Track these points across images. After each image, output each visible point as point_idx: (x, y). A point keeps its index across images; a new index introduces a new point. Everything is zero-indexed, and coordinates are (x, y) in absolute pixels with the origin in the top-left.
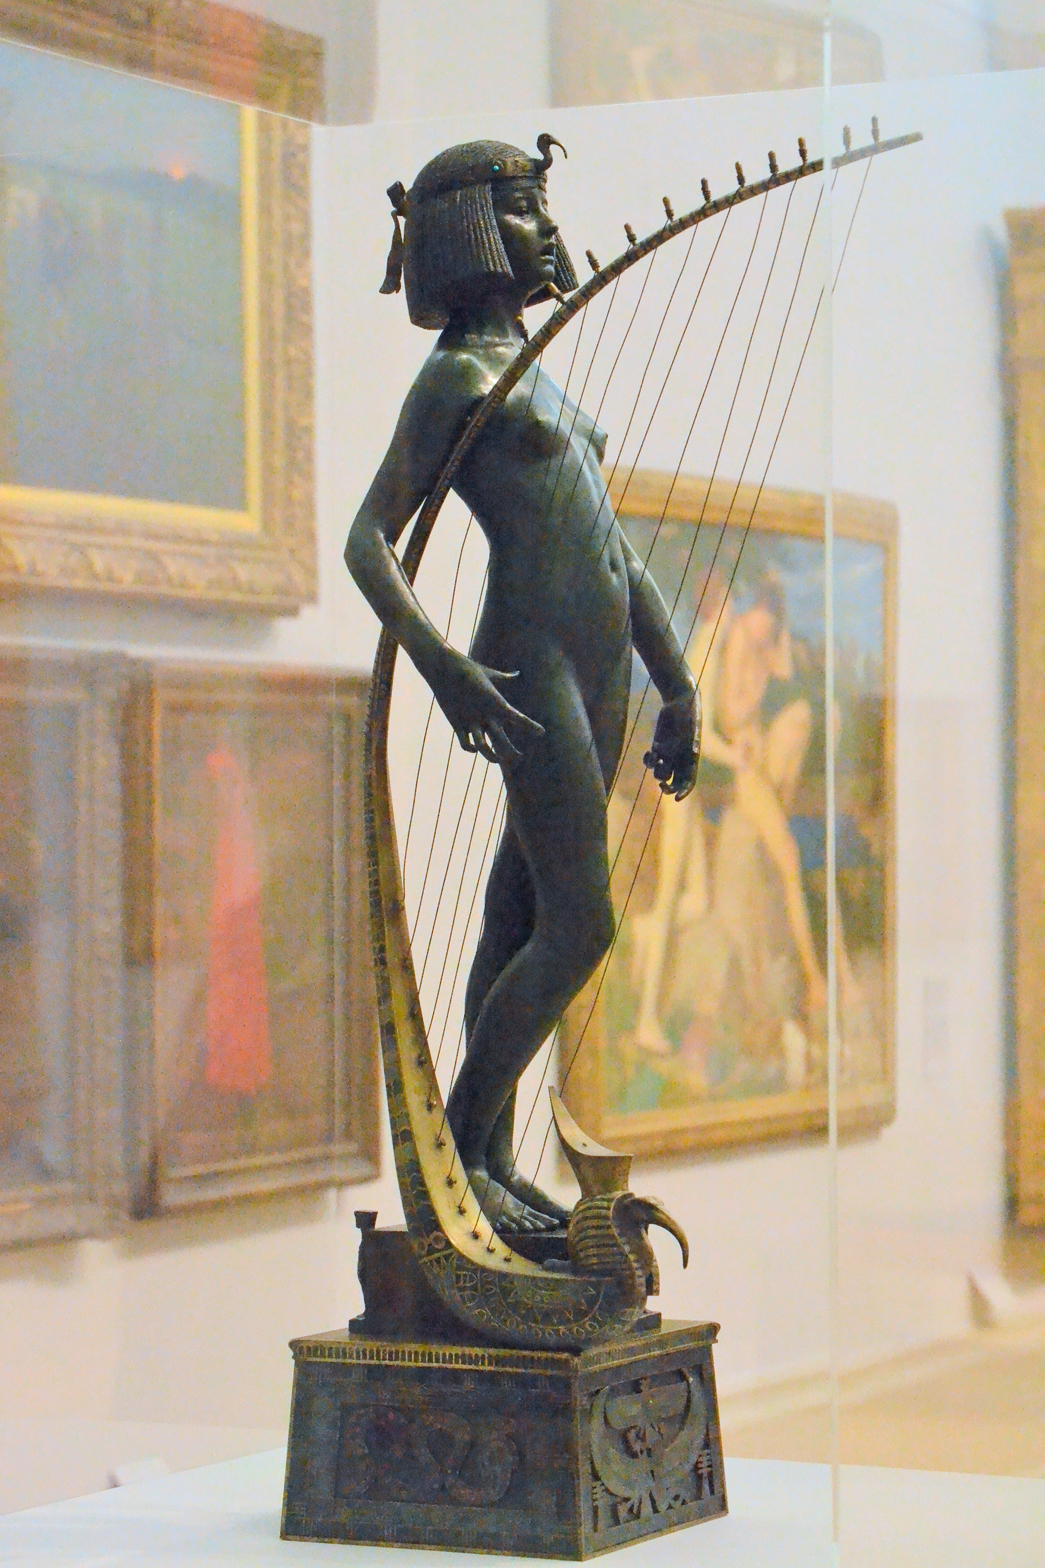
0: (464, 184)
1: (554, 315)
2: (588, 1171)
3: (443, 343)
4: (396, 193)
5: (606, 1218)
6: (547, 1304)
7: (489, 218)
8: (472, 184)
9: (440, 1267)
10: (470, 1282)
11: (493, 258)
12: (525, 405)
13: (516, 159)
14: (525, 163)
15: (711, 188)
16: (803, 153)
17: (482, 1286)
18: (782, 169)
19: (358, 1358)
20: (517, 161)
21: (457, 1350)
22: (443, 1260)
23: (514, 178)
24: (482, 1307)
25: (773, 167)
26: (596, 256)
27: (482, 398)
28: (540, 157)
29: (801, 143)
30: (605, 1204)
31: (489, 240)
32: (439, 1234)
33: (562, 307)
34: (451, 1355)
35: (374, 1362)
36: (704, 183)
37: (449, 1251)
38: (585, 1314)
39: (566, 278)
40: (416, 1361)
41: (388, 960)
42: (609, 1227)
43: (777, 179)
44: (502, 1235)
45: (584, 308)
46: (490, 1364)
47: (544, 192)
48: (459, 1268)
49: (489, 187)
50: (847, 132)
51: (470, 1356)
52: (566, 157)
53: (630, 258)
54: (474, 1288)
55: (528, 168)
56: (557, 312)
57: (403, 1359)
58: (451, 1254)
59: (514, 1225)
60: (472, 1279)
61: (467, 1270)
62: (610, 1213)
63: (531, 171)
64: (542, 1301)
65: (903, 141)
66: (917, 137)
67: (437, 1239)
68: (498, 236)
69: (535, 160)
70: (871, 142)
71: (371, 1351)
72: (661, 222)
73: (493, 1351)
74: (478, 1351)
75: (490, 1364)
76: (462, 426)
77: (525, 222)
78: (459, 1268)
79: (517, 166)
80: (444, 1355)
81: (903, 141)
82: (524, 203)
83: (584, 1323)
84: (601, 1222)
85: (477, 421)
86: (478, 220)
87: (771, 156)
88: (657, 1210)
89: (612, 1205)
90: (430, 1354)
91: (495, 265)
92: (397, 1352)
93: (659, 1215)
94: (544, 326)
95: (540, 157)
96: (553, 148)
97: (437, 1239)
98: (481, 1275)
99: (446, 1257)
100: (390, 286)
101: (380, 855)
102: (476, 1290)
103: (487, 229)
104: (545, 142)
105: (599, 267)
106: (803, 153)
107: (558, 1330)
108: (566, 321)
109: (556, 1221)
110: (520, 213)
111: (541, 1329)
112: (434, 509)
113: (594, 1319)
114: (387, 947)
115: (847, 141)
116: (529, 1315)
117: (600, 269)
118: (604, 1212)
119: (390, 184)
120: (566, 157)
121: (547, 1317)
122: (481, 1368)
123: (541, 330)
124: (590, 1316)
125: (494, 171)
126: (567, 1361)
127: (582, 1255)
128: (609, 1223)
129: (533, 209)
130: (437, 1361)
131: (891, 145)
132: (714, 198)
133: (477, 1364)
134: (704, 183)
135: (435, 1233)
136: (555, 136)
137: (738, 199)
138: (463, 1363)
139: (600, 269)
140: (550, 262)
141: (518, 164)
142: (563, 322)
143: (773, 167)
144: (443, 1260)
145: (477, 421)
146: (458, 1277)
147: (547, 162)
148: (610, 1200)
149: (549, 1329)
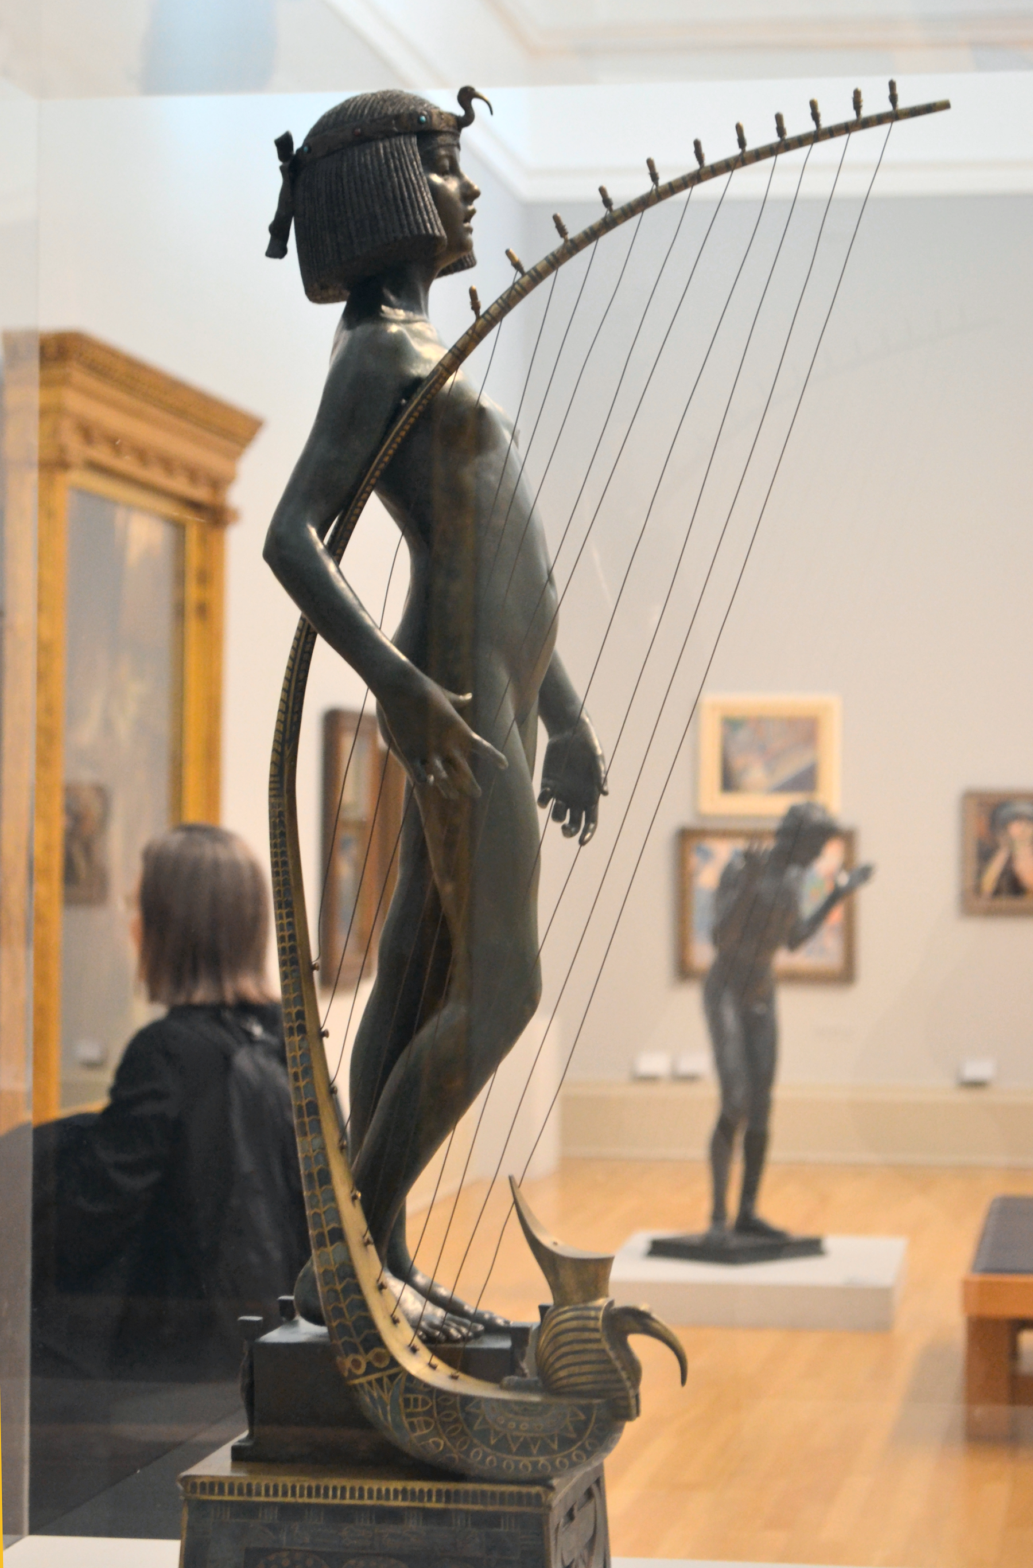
0: (388, 135)
1: (514, 284)
2: (568, 1277)
3: (350, 319)
4: (284, 144)
5: (596, 1330)
6: (526, 1431)
8: (399, 134)
9: (383, 1390)
10: (423, 1406)
11: (430, 219)
12: (459, 391)
15: (705, 150)
16: (815, 116)
17: (438, 1413)
18: (792, 131)
19: (267, 1494)
21: (398, 1485)
22: (385, 1380)
23: (439, 133)
24: (439, 1435)
25: (781, 131)
26: (564, 221)
27: (418, 381)
28: (460, 112)
29: (813, 105)
30: (593, 1313)
32: (383, 1351)
34: (388, 1491)
35: (289, 1499)
36: (697, 144)
38: (572, 1442)
40: (343, 1497)
41: (308, 1029)
42: (598, 1341)
43: (785, 145)
44: (433, 1346)
46: (438, 1501)
48: (408, 1390)
49: (414, 140)
50: (857, 96)
51: (413, 1492)
52: (492, 113)
53: (608, 224)
54: (429, 1413)
57: (326, 1496)
58: (396, 1375)
59: (438, 1333)
60: (425, 1403)
62: (600, 1323)
64: (517, 1428)
66: (945, 106)
68: (430, 196)
70: (887, 107)
71: (285, 1486)
72: (645, 186)
73: (444, 1486)
74: (425, 1486)
75: (438, 1501)
76: (398, 411)
78: (408, 1390)
79: (442, 119)
80: (379, 1491)
82: (447, 163)
83: (572, 1453)
84: (586, 1335)
85: (414, 405)
87: (779, 118)
88: (653, 1319)
89: (601, 1314)
90: (361, 1489)
92: (318, 1488)
93: (654, 1325)
94: (501, 297)
95: (460, 112)
96: (475, 103)
97: (379, 1358)
98: (437, 1398)
99: (392, 1378)
100: (276, 250)
101: (294, 904)
102: (432, 1417)
103: (420, 187)
104: (466, 96)
106: (815, 116)
107: (537, 1463)
109: (480, 1327)
110: (442, 173)
111: (484, 1452)
112: (360, 504)
113: (582, 1448)
114: (306, 1013)
116: (502, 1445)
117: (570, 236)
118: (592, 1324)
119: (279, 134)
121: (524, 1449)
122: (428, 1505)
123: (497, 302)
124: (579, 1443)
125: (420, 122)
126: (538, 1496)
127: (562, 1374)
128: (597, 1335)
129: (453, 170)
130: (371, 1497)
132: (709, 160)
133: (421, 1500)
134: (697, 144)
135: (377, 1350)
136: (478, 90)
137: (740, 163)
138: (404, 1499)
139: (570, 236)
141: (443, 117)
143: (781, 131)
144: (385, 1380)
145: (414, 405)
146: (407, 1401)
147: (468, 119)
148: (598, 1309)
149: (525, 1461)
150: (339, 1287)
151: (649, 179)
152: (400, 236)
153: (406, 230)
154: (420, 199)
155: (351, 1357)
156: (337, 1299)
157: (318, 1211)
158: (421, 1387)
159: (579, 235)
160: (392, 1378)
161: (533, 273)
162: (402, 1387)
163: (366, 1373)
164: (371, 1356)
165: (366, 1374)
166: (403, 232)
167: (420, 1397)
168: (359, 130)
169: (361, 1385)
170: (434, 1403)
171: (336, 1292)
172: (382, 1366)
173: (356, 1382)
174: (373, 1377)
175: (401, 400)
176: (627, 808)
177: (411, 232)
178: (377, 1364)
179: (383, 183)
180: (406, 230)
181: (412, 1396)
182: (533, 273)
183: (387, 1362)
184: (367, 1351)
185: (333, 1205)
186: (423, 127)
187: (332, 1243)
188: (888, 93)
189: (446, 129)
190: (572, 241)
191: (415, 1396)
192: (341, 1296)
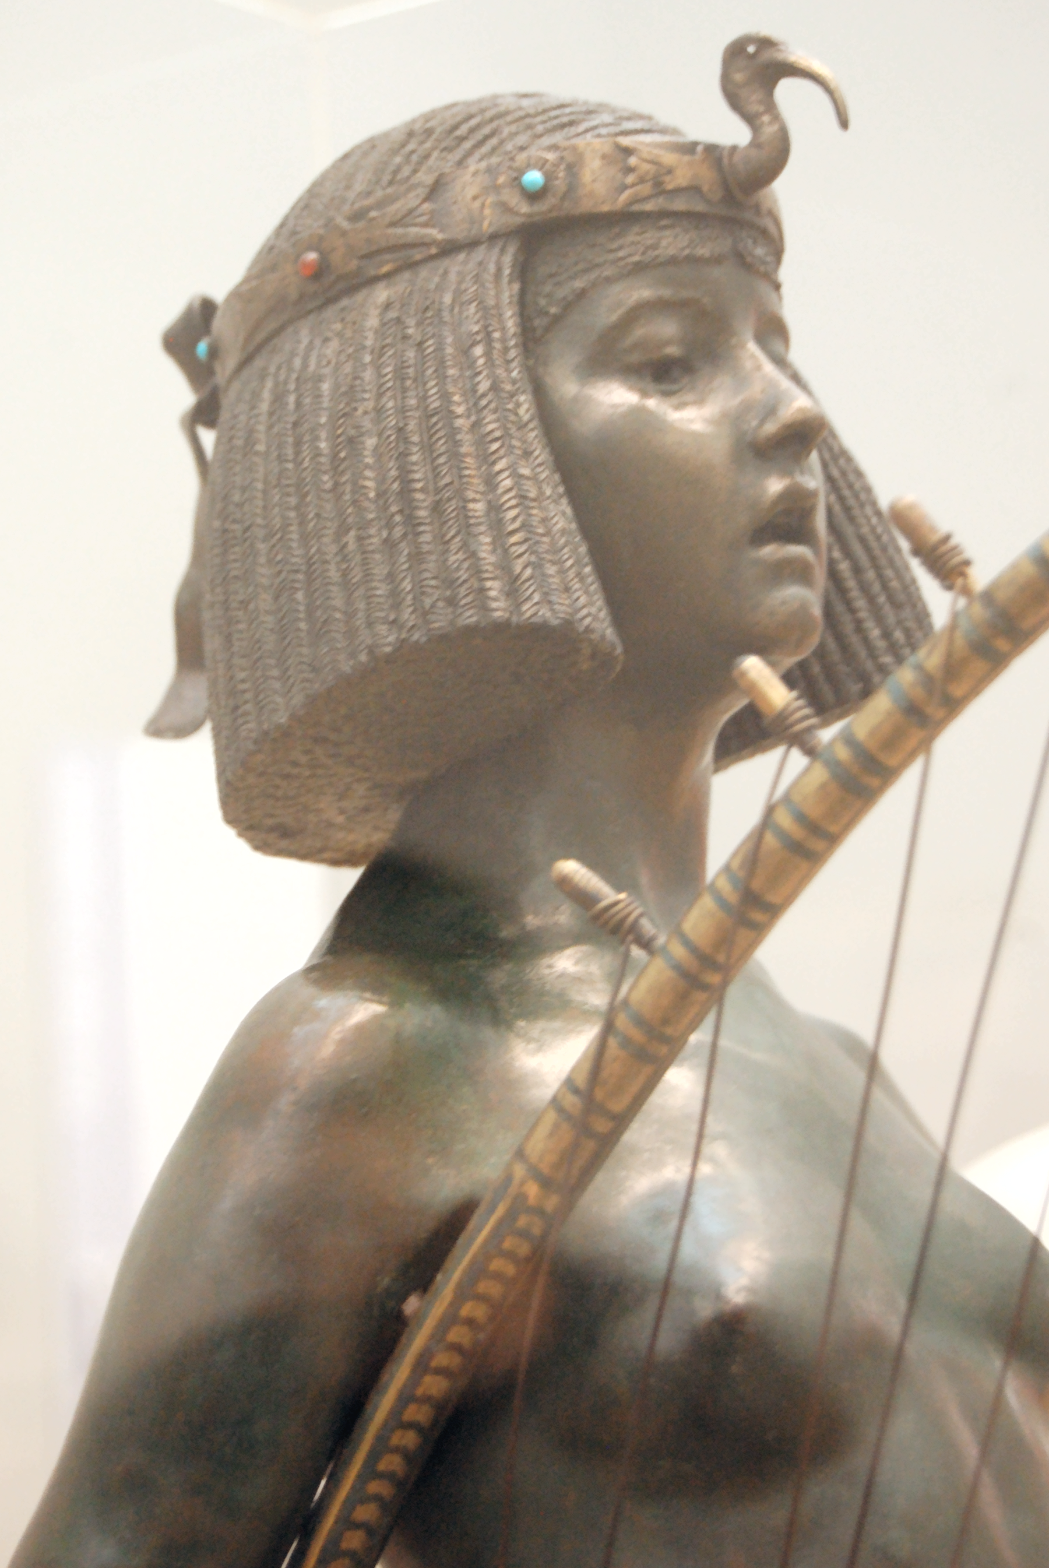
1: (770, 811)
7: (495, 388)
11: (505, 567)
13: (626, 141)
14: (669, 158)
20: (628, 151)
31: (491, 482)
33: (806, 771)
39: (886, 635)
45: (910, 776)
47: (773, 295)
52: (844, 124)
55: (681, 178)
56: (787, 798)
63: (694, 189)
69: (711, 150)
77: (679, 407)
86: (445, 396)
91: (513, 590)
103: (482, 441)
105: (967, 563)
108: (833, 840)
120: (844, 124)
125: (534, 196)
140: (801, 573)
141: (633, 161)
142: (818, 845)
152: (388, 639)
153: (407, 615)
154: (475, 488)
159: (1014, 567)
161: (843, 753)
168: (312, 256)
175: (404, 1298)
182: (843, 753)
186: (542, 207)
189: (649, 207)
190: (988, 597)
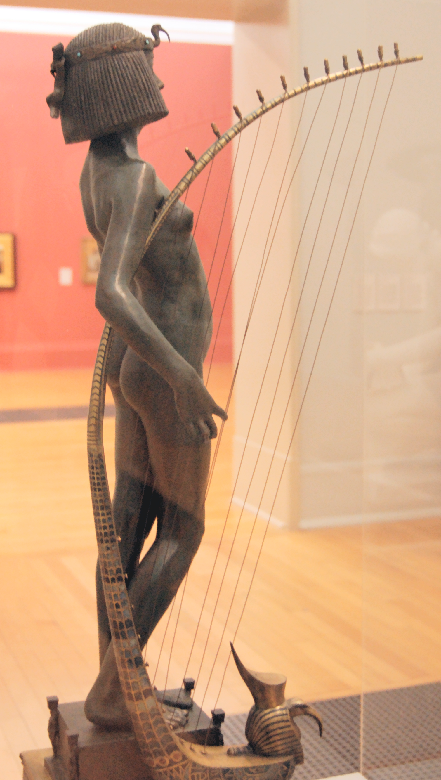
5: (287, 721)
22: (181, 768)
37: (185, 762)
42: (289, 726)
48: (193, 771)
61: (200, 771)
65: (414, 60)
67: (176, 757)
81: (414, 60)
98: (210, 772)
99: (184, 766)
115: (381, 56)
131: (408, 61)
135: (175, 752)
136: (163, 27)
144: (181, 768)
150: (151, 721)
151: (282, 87)
155: (159, 758)
156: (151, 727)
157: (136, 680)
158: (200, 768)
160: (184, 766)
162: (190, 770)
163: (170, 765)
164: (172, 756)
165: (170, 765)
166: (152, 109)
167: (200, 774)
169: (166, 773)
170: (208, 776)
171: (150, 725)
172: (178, 760)
173: (161, 770)
174: (173, 767)
176: (251, 429)
177: (156, 109)
178: (176, 760)
179: (137, 80)
180: (154, 108)
181: (195, 774)
183: (180, 758)
184: (169, 753)
185: (145, 676)
187: (146, 697)
188: (393, 50)
191: (198, 773)
192: (153, 726)
